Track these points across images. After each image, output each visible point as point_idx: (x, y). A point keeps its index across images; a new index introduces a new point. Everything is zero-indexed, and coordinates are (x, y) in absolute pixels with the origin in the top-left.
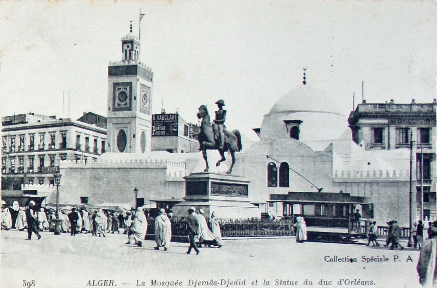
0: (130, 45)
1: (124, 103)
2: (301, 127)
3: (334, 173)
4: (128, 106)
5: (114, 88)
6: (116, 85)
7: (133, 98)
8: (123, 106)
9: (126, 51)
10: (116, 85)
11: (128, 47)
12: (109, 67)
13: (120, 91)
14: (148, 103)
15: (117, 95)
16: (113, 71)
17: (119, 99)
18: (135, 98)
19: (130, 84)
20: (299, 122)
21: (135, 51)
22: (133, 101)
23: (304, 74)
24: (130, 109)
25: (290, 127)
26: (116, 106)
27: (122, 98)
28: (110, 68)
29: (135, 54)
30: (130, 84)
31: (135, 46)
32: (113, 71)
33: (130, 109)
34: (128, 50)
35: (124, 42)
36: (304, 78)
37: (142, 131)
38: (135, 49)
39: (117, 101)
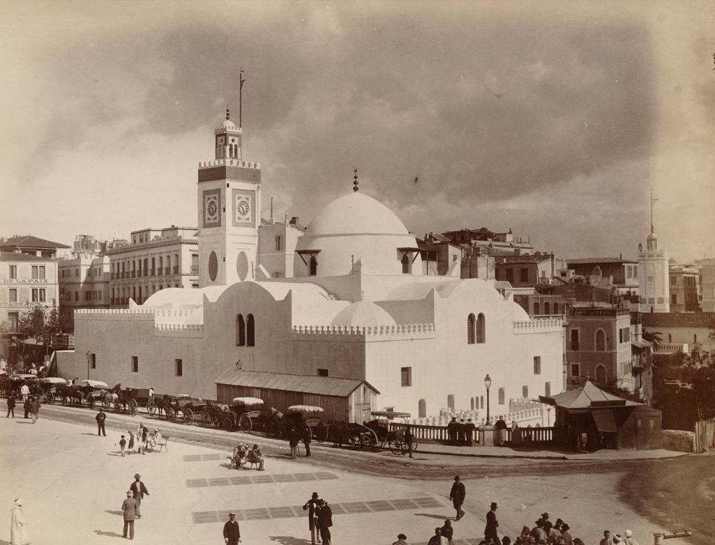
1: (214, 216)
2: (319, 258)
4: (217, 221)
5: (204, 198)
6: (206, 193)
8: (212, 221)
10: (206, 193)
11: (222, 141)
12: (199, 171)
14: (250, 212)
16: (208, 175)
17: (209, 212)
19: (218, 191)
20: (317, 252)
21: (231, 145)
22: (222, 213)
23: (356, 177)
24: (219, 224)
25: (307, 257)
26: (207, 221)
27: (212, 211)
28: (200, 171)
29: (231, 149)
30: (218, 191)
31: (230, 138)
32: (208, 175)
33: (219, 224)
35: (217, 136)
36: (355, 183)
37: (239, 251)
38: (230, 142)
39: (207, 215)
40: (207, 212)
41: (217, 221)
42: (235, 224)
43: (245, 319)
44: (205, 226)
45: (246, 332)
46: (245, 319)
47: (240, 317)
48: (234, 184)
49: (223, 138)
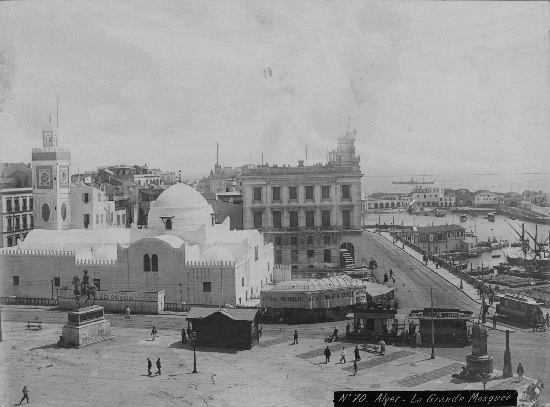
0: (50, 134)
2: (173, 221)
3: (186, 262)
4: (49, 185)
7: (53, 178)
9: (46, 138)
13: (42, 173)
15: (40, 175)
17: (42, 179)
18: (55, 179)
22: (54, 180)
24: (51, 187)
25: (165, 220)
28: (33, 154)
30: (50, 167)
31: (54, 134)
33: (51, 187)
34: (48, 137)
38: (54, 136)
40: (40, 179)
41: (49, 185)
42: (61, 187)
43: (151, 257)
44: (39, 187)
45: (151, 263)
46: (151, 257)
47: (146, 257)
48: (60, 163)
49: (50, 134)
